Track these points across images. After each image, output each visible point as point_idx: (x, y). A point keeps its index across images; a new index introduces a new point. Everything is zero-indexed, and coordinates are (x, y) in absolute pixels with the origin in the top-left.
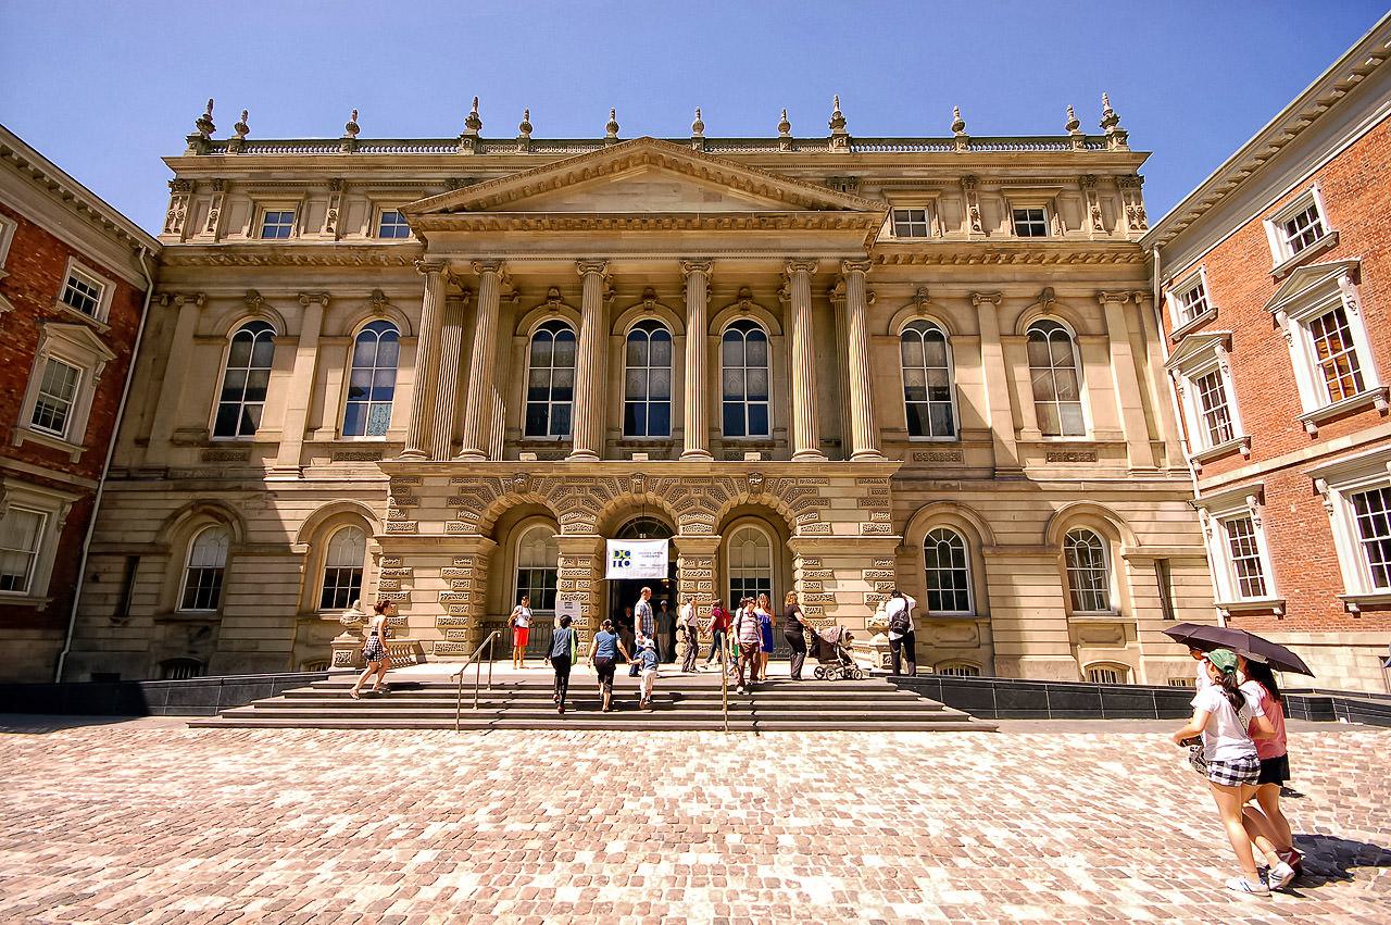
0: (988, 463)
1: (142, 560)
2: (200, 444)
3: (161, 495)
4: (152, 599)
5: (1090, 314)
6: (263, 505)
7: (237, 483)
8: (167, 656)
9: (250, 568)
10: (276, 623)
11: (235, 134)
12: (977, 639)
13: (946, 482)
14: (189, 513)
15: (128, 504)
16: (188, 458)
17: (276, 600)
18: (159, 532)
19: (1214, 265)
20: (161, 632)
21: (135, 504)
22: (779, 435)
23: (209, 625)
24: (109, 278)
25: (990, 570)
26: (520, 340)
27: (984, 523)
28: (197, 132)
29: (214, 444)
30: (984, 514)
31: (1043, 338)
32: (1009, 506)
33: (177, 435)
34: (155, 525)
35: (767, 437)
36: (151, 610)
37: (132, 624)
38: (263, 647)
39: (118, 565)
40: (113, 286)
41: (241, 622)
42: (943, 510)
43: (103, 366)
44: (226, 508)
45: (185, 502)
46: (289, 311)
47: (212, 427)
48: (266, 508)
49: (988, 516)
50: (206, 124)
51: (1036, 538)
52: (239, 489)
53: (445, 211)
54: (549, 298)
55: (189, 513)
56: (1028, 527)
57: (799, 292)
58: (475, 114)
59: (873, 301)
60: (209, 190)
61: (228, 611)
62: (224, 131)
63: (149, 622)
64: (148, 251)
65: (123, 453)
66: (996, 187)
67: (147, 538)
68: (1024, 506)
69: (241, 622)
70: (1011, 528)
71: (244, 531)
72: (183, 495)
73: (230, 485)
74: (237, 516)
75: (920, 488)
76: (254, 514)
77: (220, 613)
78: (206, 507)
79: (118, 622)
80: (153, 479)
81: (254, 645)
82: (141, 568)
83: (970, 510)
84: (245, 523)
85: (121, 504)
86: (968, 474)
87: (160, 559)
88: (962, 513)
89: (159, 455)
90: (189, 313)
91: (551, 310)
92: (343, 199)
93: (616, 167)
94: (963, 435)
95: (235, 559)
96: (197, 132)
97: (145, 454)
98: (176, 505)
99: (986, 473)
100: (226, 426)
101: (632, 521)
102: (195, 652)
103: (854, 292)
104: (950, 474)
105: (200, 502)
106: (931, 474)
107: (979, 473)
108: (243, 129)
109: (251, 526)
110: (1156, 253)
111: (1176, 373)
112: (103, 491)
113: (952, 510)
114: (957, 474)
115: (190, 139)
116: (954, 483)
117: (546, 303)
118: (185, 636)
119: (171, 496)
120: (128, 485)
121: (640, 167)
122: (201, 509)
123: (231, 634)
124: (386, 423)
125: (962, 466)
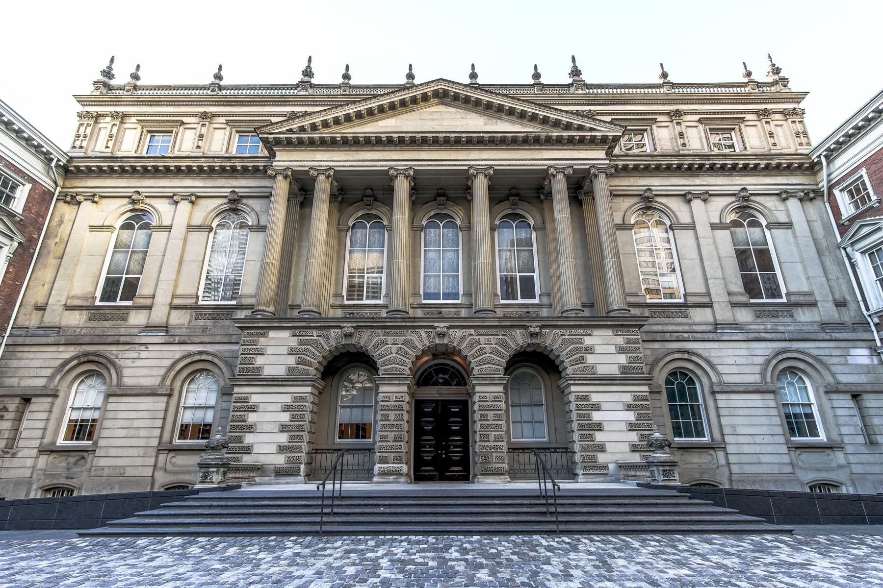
0: (711, 320)
1: (34, 400)
2: (87, 308)
3: (54, 348)
4: (39, 433)
5: (776, 207)
6: (135, 355)
7: (116, 338)
8: (48, 482)
9: (122, 406)
10: (141, 452)
11: (129, 80)
12: (715, 460)
13: (679, 334)
15: (25, 355)
17: (142, 433)
18: (51, 378)
19: (874, 168)
20: (43, 460)
21: (31, 356)
22: (545, 300)
23: (85, 454)
24: (26, 180)
25: (721, 404)
27: (712, 366)
28: (101, 78)
29: (99, 308)
30: (711, 359)
31: (742, 226)
32: (730, 352)
33: (69, 301)
34: (49, 372)
35: (536, 301)
36: (36, 443)
37: (20, 455)
38: (129, 472)
39: (13, 405)
40: (29, 186)
41: (113, 452)
42: (679, 356)
43: (16, 244)
44: (106, 358)
45: (73, 354)
46: (163, 206)
47: (98, 294)
48: (138, 358)
49: (714, 361)
50: (108, 73)
51: (757, 378)
52: (118, 343)
53: (290, 131)
54: (366, 196)
55: (75, 362)
56: (747, 369)
60: (108, 119)
61: (102, 443)
62: (121, 77)
63: (34, 452)
64: (59, 160)
65: (26, 315)
66: (697, 117)
67: (41, 382)
68: (743, 352)
69: (113, 452)
70: (734, 369)
71: (120, 377)
72: (72, 348)
73: (109, 340)
74: (114, 364)
75: (658, 339)
76: (129, 363)
77: (95, 444)
79: (7, 453)
80: (48, 336)
81: (122, 471)
83: (699, 356)
84: (121, 372)
85: (19, 355)
86: (695, 328)
87: (49, 400)
88: (694, 358)
89: (52, 317)
90: (86, 206)
91: (367, 205)
92: (209, 126)
94: (689, 298)
95: (111, 399)
96: (101, 78)
97: (43, 316)
98: (67, 356)
99: (710, 328)
101: (430, 367)
102: (72, 478)
104: (680, 328)
105: (85, 354)
106: (666, 328)
107: (703, 328)
108: (135, 77)
109: (126, 372)
110: (823, 159)
111: (849, 249)
112: (6, 345)
113: (686, 356)
114: (687, 328)
115: (95, 83)
116: (686, 335)
118: (65, 465)
119: (61, 348)
120: (28, 340)
123: (103, 462)
125: (690, 321)
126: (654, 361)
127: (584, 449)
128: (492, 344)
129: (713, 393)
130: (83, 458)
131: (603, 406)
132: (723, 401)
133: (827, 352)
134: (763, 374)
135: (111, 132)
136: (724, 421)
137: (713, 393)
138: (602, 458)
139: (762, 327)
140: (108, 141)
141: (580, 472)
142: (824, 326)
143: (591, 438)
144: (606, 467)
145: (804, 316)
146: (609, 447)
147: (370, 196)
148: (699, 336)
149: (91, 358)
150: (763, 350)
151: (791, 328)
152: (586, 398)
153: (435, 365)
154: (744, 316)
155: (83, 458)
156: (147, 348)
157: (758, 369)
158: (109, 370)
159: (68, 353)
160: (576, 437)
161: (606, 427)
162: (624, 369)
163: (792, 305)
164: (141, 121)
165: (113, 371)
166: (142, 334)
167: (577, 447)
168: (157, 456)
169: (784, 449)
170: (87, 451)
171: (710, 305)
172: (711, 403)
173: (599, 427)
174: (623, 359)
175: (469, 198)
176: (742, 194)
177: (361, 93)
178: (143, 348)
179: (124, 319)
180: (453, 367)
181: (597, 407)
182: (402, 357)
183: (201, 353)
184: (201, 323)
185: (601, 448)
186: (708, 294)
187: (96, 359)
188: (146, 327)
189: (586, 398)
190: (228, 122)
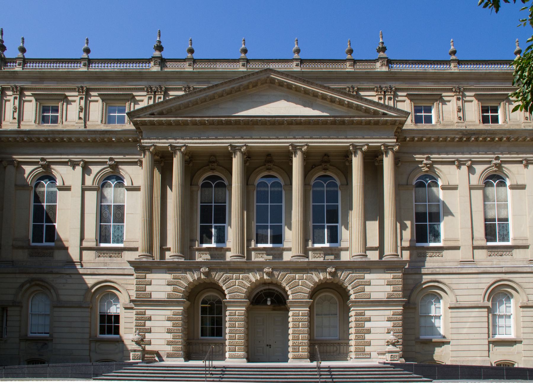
1: (9, 309)
14: (28, 285)
16: (21, 255)
26: (195, 188)
44: (47, 283)
52: (52, 273)
55: (28, 285)
57: (357, 162)
58: (160, 42)
59: (400, 164)
71: (58, 295)
78: (38, 282)
82: (9, 313)
93: (251, 86)
98: (22, 281)
100: (37, 238)
103: (388, 162)
105: (33, 280)
117: (208, 165)
119: (18, 276)
121: (264, 85)
122: (33, 283)
124: (122, 236)
126: (414, 287)
128: (303, 279)
130: (46, 344)
133: (527, 280)
135: (14, 104)
139: (490, 263)
140: (14, 112)
147: (214, 162)
148: (447, 271)
149: (38, 282)
153: (265, 290)
155: (46, 344)
156: (71, 276)
158: (50, 290)
159: (23, 278)
164: (35, 94)
165: (52, 291)
166: (65, 267)
168: (90, 344)
170: (48, 340)
175: (290, 164)
176: (495, 162)
177: (203, 67)
178: (68, 276)
179: (51, 255)
180: (276, 291)
182: (241, 288)
183: (106, 281)
184: (102, 259)
187: (41, 283)
188: (67, 262)
190: (100, 95)
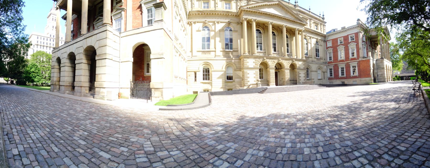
0: (311, 60)
25: (312, 73)
27: (311, 68)
49: (312, 67)
51: (315, 70)
127: (298, 80)
129: (311, 72)
131: (301, 74)
132: (312, 73)
134: (316, 69)
136: (312, 76)
137: (311, 72)
138: (300, 81)
141: (298, 83)
142: (323, 63)
143: (299, 78)
144: (300, 83)
145: (322, 61)
146: (301, 80)
150: (317, 65)
151: (320, 62)
152: (299, 72)
154: (315, 60)
157: (316, 68)
160: (297, 78)
161: (301, 77)
162: (304, 68)
163: (320, 59)
167: (297, 80)
169: (317, 80)
171: (311, 57)
172: (310, 73)
173: (300, 77)
174: (304, 66)
181: (300, 74)
185: (300, 80)
186: (312, 56)
189: (299, 72)
